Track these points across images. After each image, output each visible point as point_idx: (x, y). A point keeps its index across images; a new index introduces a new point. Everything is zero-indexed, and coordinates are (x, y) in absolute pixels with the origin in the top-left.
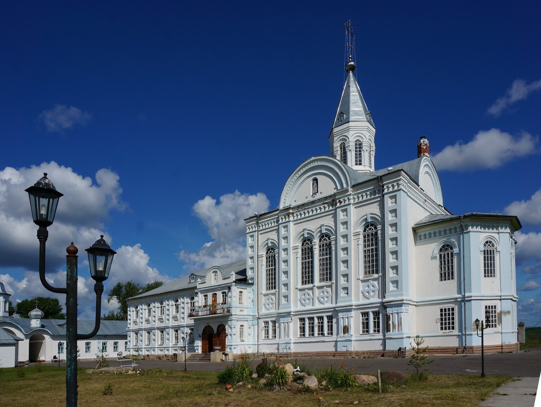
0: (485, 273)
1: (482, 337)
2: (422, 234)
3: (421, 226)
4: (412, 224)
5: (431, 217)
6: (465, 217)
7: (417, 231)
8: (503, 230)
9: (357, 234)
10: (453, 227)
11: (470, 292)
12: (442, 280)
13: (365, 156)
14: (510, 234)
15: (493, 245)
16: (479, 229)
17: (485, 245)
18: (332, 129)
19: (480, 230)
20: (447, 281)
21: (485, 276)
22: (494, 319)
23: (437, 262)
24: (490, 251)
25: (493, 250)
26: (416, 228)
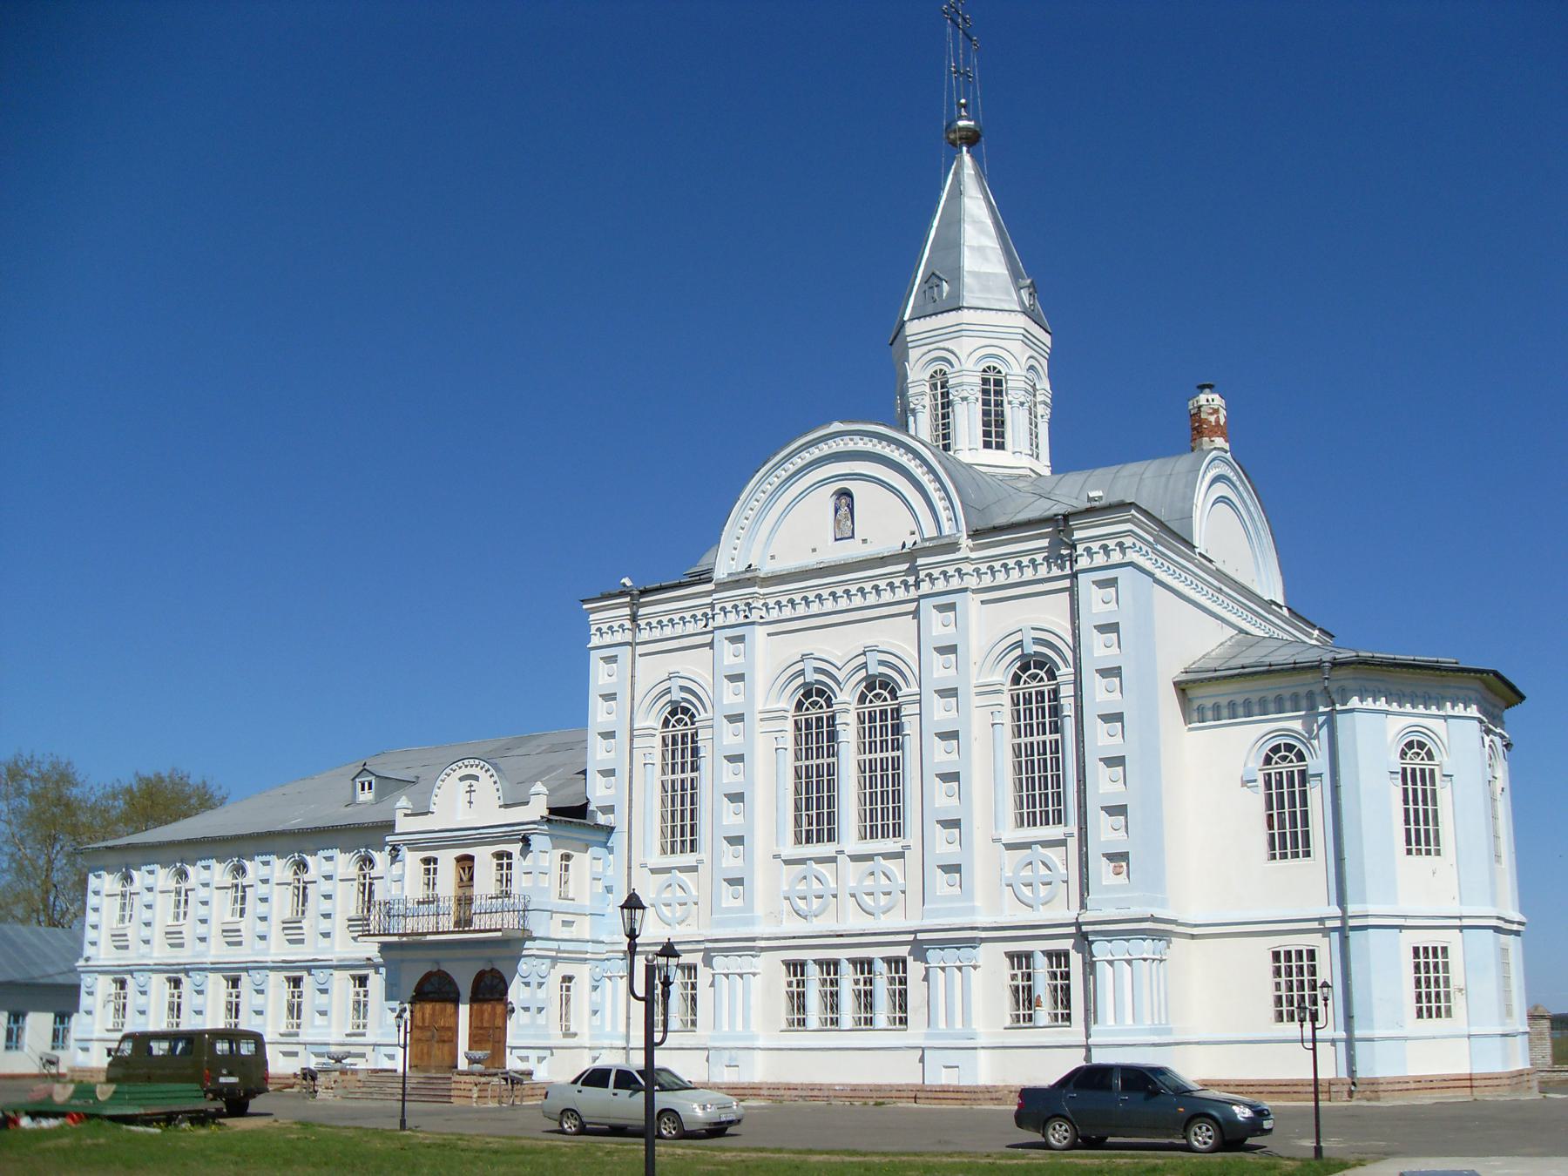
0: (1408, 842)
1: (1314, 1049)
2: (1209, 703)
3: (1202, 680)
4: (1174, 669)
5: (1238, 643)
6: (1336, 664)
7: (1191, 693)
8: (1459, 709)
9: (991, 690)
10: (1303, 691)
11: (1363, 901)
12: (1273, 857)
13: (1017, 422)
14: (1481, 721)
15: (1430, 755)
16: (1382, 704)
17: (1403, 754)
18: (903, 324)
19: (1386, 707)
20: (1290, 862)
21: (1409, 852)
22: (1433, 990)
23: (1257, 798)
24: (1423, 771)
25: (1432, 771)
26: (1187, 682)
